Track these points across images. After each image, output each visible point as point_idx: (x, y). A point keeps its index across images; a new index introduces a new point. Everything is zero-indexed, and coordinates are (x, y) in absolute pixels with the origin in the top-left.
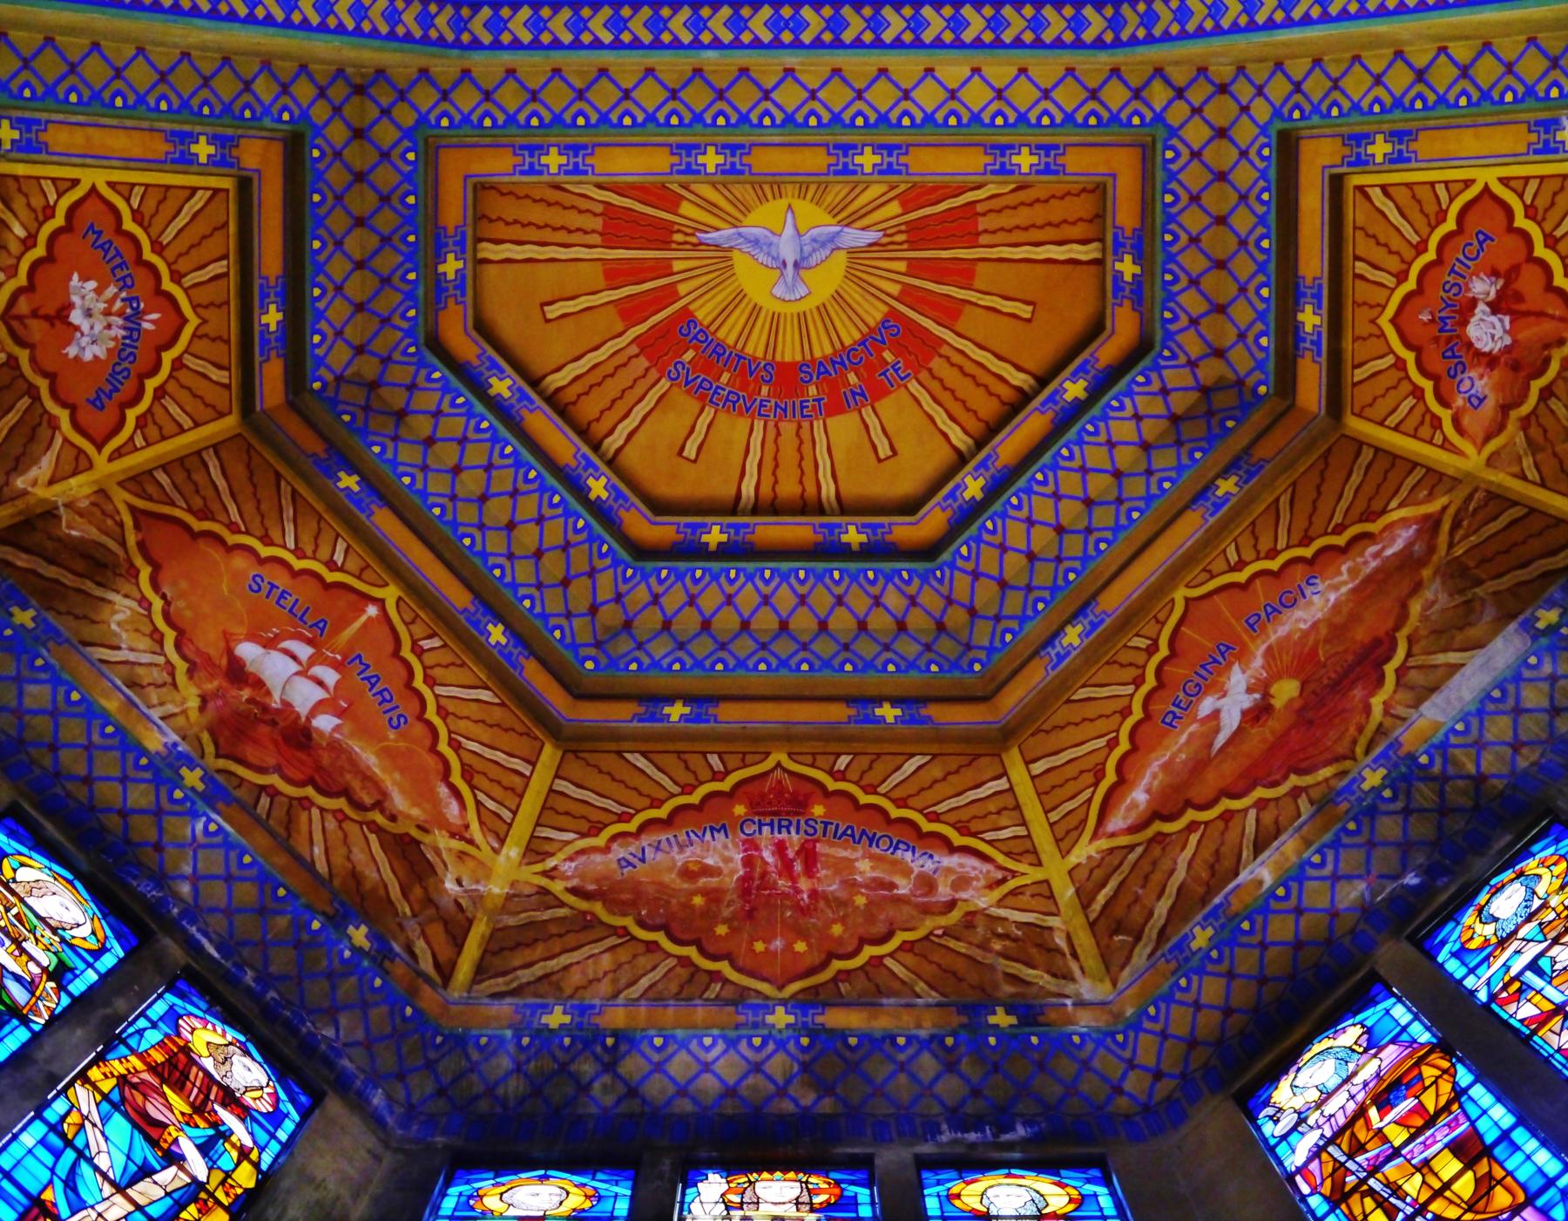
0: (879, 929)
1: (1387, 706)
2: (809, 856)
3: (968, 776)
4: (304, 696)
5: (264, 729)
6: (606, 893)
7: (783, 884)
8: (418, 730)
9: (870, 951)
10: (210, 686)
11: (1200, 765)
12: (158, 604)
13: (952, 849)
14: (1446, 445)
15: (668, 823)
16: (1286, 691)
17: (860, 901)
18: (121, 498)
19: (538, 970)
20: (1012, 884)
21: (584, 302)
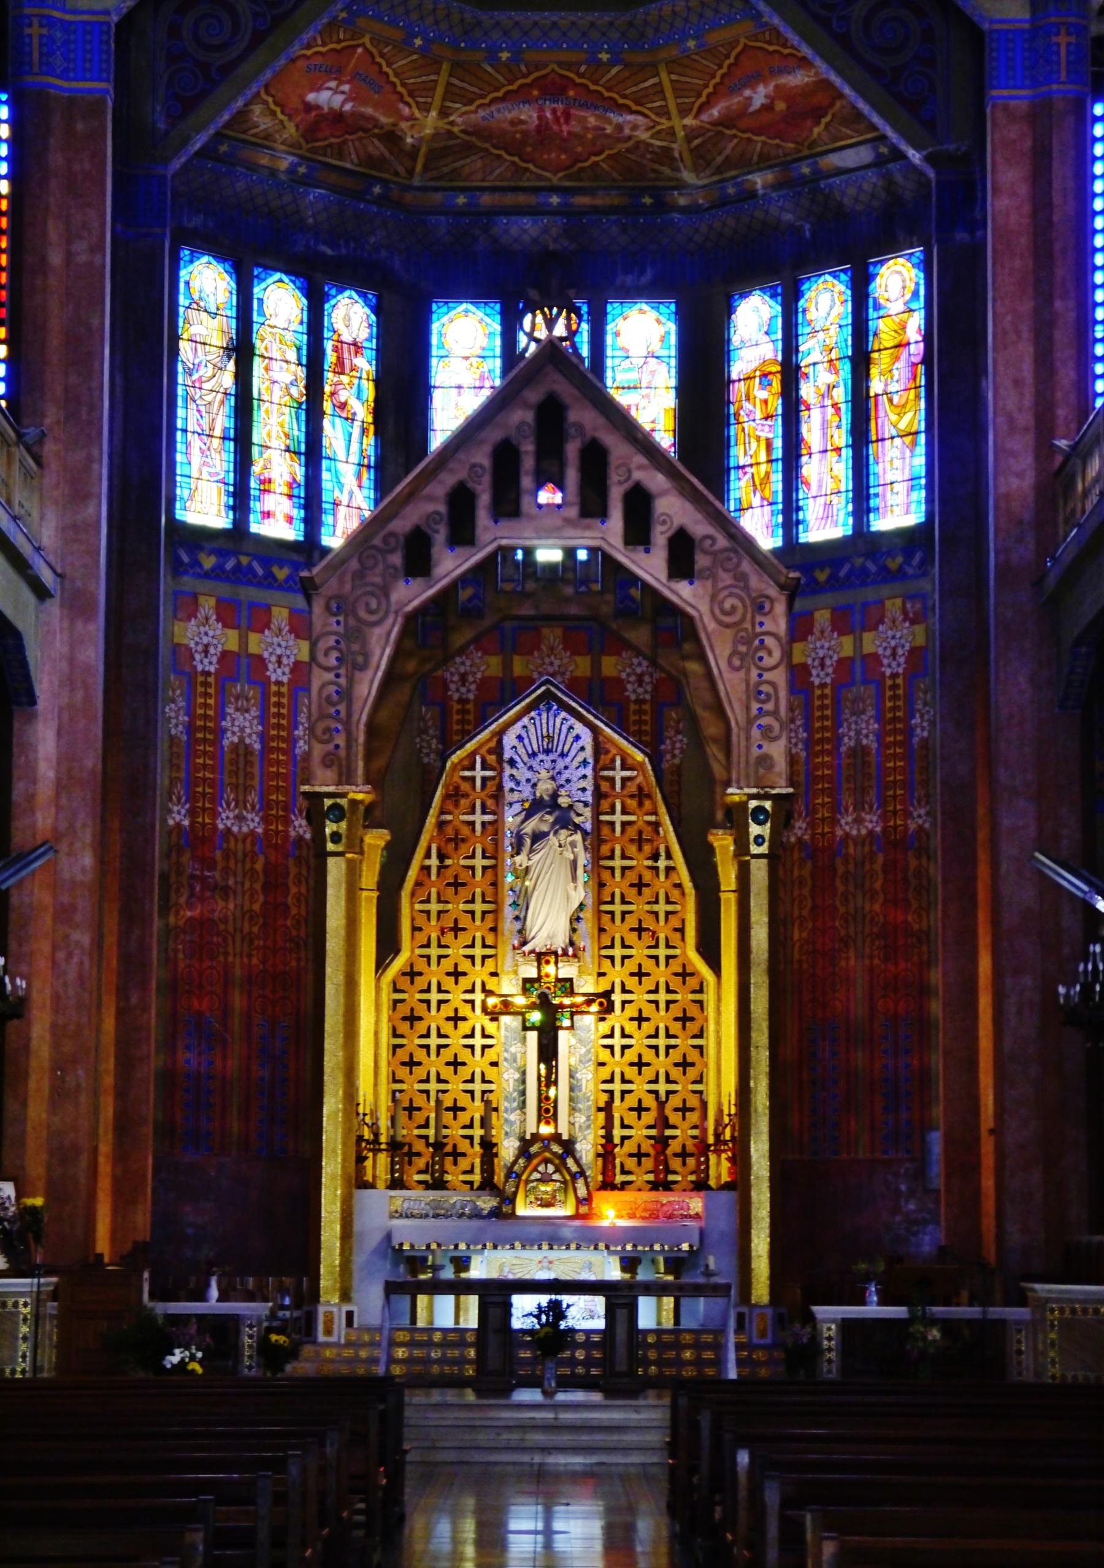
1: (819, 135)
2: (567, 116)
6: (476, 131)
7: (555, 128)
8: (388, 88)
9: (594, 159)
10: (298, 119)
12: (270, 100)
13: (632, 112)
15: (503, 99)
16: (781, 106)
17: (590, 136)
20: (658, 128)
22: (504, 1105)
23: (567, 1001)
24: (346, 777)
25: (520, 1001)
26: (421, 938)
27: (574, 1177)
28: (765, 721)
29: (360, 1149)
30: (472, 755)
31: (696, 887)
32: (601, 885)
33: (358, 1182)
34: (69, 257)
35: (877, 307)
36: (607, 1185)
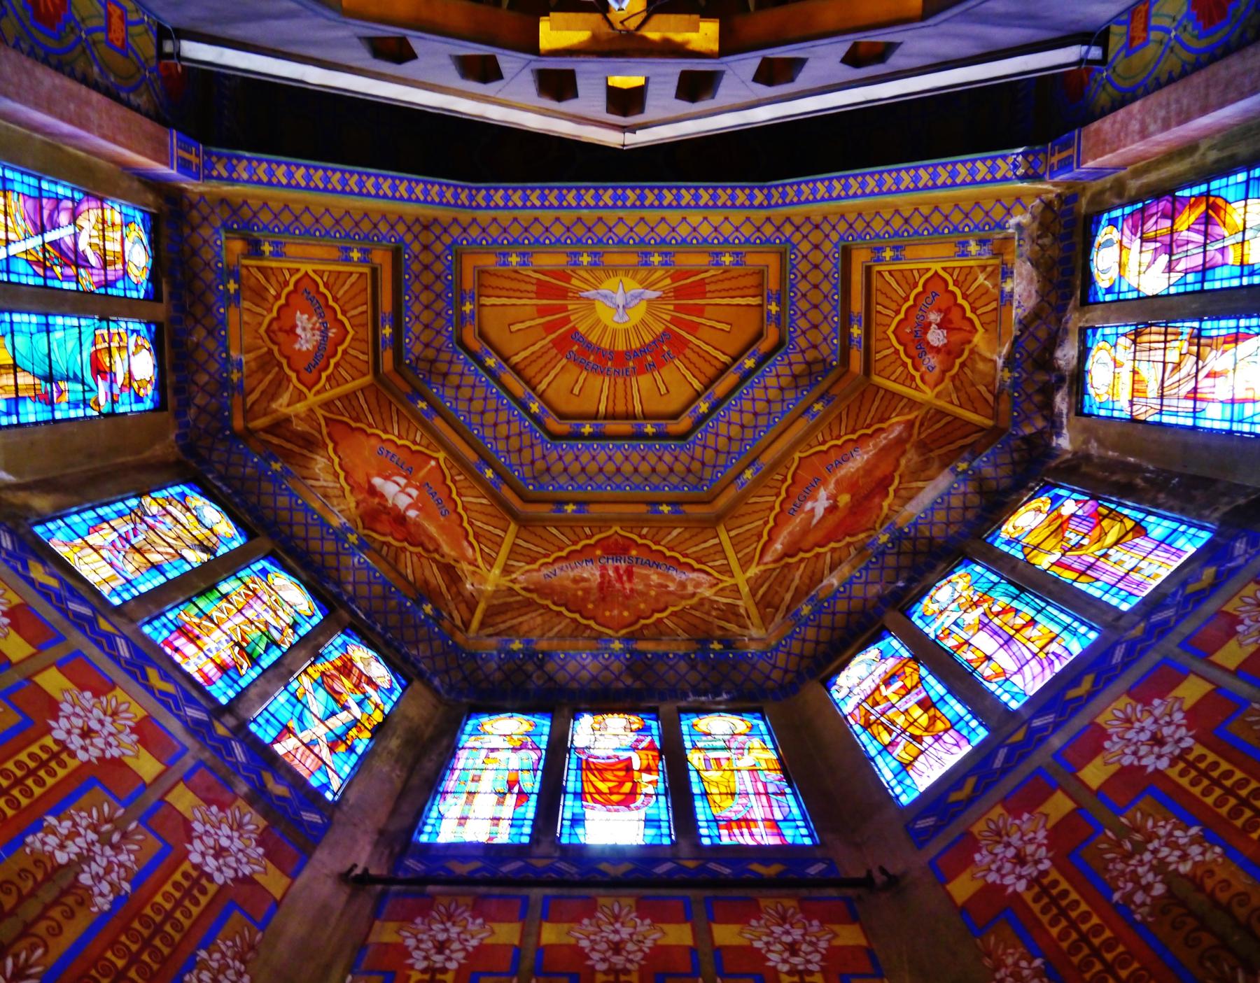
0: (662, 605)
2: (630, 574)
3: (700, 538)
4: (403, 501)
5: (384, 517)
6: (539, 589)
8: (454, 516)
9: (657, 615)
10: (360, 497)
11: (806, 531)
12: (336, 460)
13: (694, 570)
14: (917, 388)
15: (566, 558)
16: (844, 499)
17: (653, 593)
18: (320, 413)
19: (508, 624)
21: (528, 324)
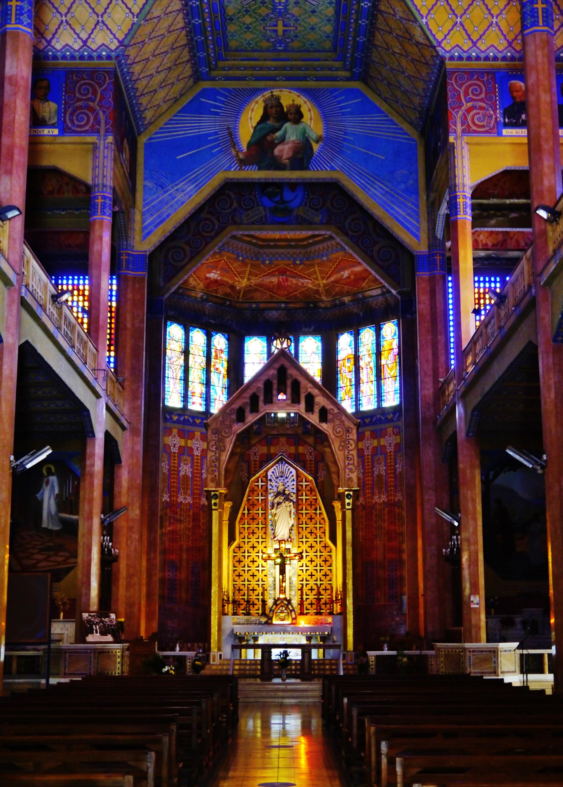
2: (287, 280)
16: (352, 277)
22: (269, 589)
23: (288, 555)
24: (218, 485)
25: (274, 556)
26: (242, 536)
27: (291, 611)
28: (350, 467)
29: (223, 603)
30: (258, 478)
31: (329, 519)
32: (299, 519)
33: (223, 613)
34: (133, 325)
35: (384, 338)
36: (302, 614)
